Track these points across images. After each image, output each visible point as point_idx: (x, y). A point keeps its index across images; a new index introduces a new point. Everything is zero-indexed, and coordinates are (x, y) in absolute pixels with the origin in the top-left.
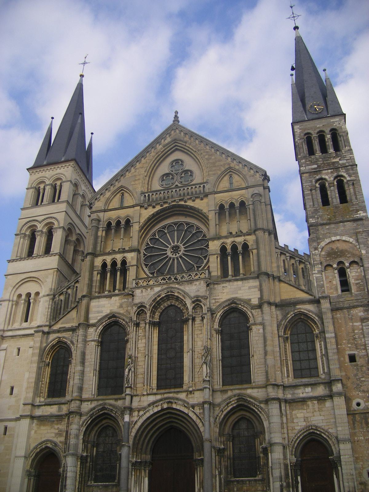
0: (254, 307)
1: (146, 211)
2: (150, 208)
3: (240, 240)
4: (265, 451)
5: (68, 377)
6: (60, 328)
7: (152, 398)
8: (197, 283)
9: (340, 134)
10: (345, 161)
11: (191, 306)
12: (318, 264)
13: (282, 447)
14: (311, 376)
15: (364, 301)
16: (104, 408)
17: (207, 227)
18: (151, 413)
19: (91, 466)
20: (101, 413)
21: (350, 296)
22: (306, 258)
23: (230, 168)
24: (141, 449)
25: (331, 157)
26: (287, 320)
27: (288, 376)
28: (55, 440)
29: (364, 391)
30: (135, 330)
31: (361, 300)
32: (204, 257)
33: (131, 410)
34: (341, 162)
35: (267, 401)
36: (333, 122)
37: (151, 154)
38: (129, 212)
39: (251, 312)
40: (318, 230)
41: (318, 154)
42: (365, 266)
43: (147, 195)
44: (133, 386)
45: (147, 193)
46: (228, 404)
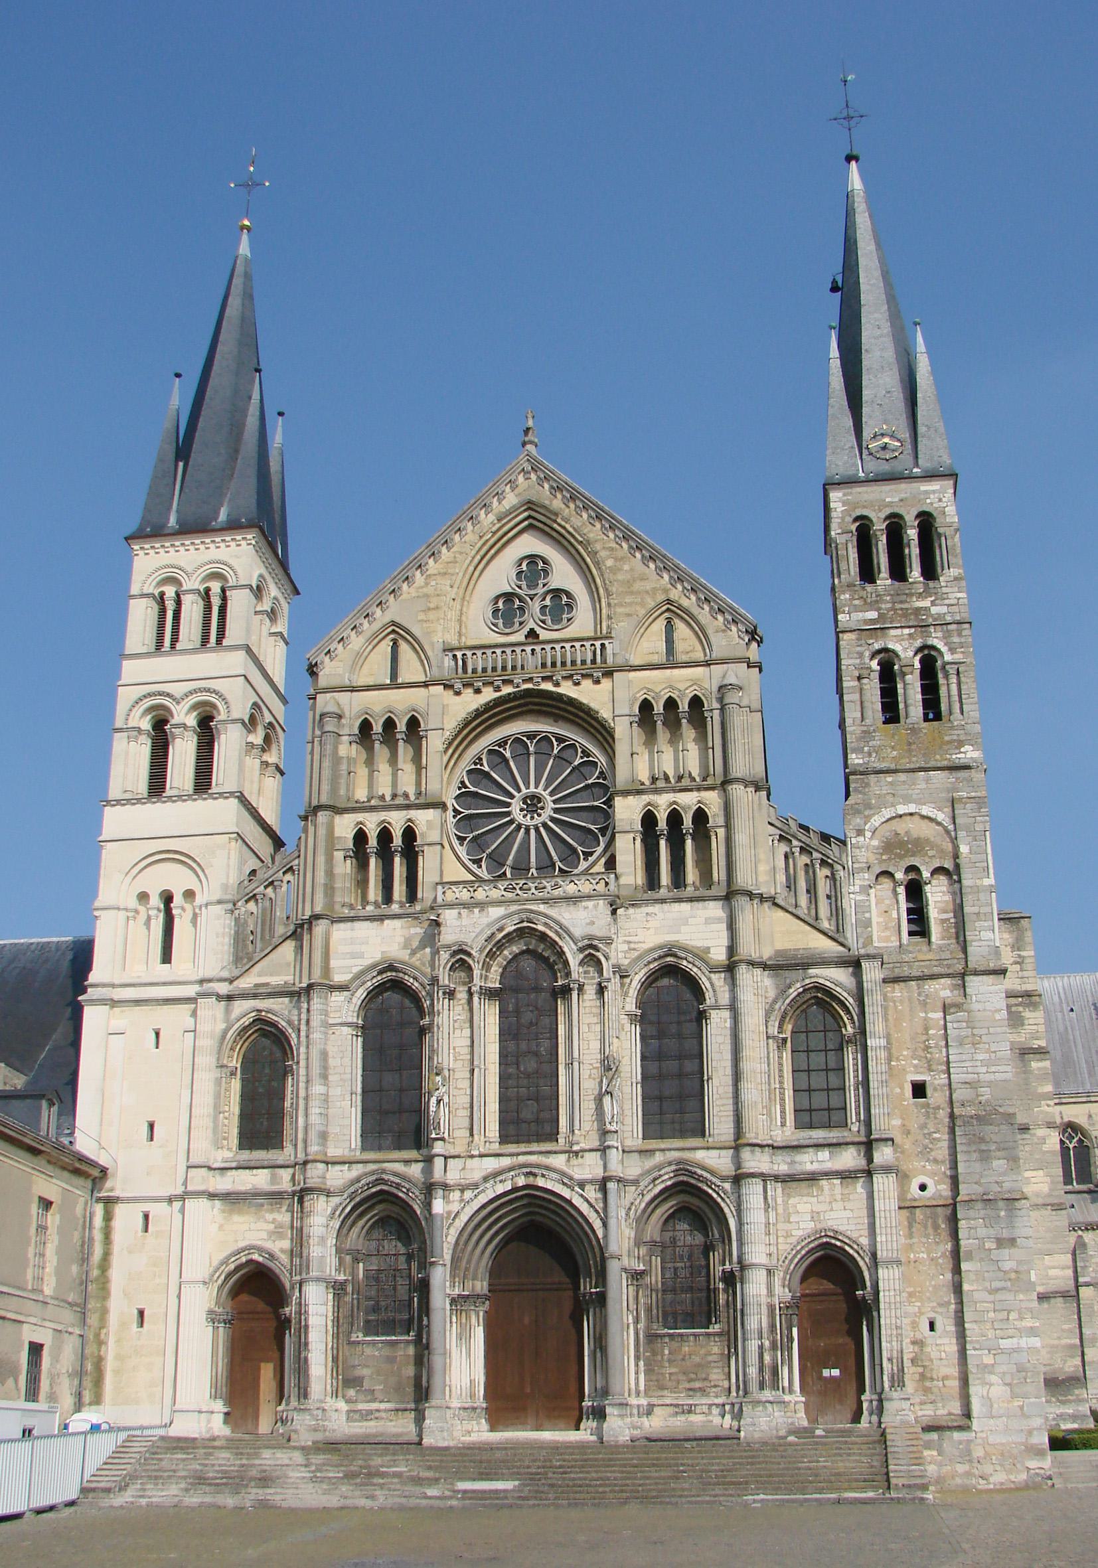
0: (714, 969)
3: (688, 801)
4: (730, 1279)
5: (287, 1104)
6: (257, 985)
7: (491, 1164)
8: (590, 904)
9: (940, 530)
10: (944, 609)
12: (861, 870)
13: (764, 1272)
14: (828, 1126)
15: (954, 965)
16: (380, 1181)
17: (609, 754)
18: (491, 1195)
19: (355, 1302)
20: (374, 1190)
21: (925, 948)
22: (837, 854)
23: (669, 601)
24: (467, 1269)
25: (911, 595)
26: (788, 1001)
27: (783, 1124)
28: (268, 1245)
29: (936, 1161)
30: (446, 1007)
31: (949, 962)
33: (445, 1187)
34: (934, 610)
35: (738, 1179)
36: (926, 492)
37: (466, 538)
38: (416, 697)
39: (709, 979)
40: (868, 785)
41: (884, 579)
42: (965, 882)
43: (459, 654)
44: (446, 1135)
45: (460, 649)
46: (655, 1179)
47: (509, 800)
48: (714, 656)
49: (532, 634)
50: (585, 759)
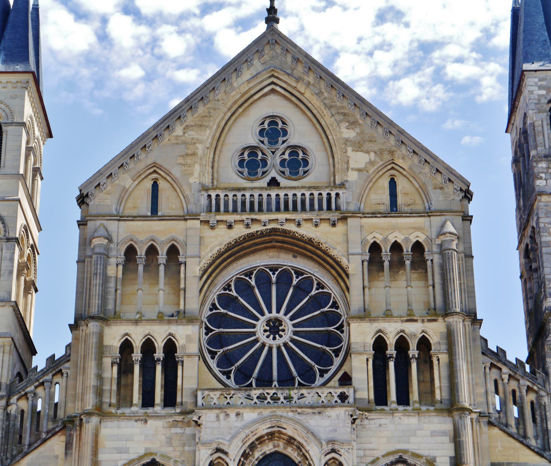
2: (222, 229)
11: (320, 460)
32: (334, 351)
37: (219, 97)
43: (213, 195)
45: (215, 189)
47: (254, 322)
48: (433, 208)
50: (320, 290)
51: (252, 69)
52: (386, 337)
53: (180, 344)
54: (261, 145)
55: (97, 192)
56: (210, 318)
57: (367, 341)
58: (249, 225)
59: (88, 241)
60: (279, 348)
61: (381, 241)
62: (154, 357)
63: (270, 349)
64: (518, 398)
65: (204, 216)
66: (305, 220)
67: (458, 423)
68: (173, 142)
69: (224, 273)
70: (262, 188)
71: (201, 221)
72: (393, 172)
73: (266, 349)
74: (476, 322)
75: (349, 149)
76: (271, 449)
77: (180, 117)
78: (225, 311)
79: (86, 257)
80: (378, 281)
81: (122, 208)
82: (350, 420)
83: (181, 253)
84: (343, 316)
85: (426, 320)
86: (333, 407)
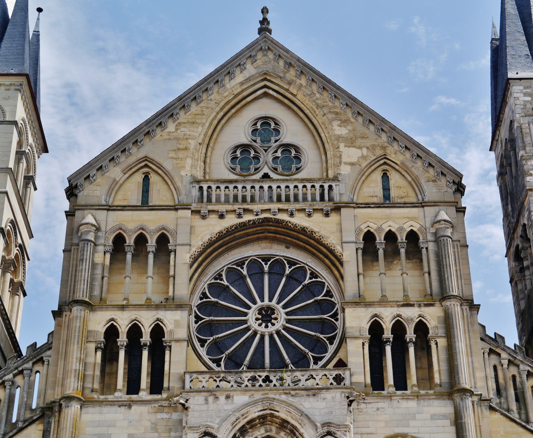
1: (203, 222)
2: (213, 219)
17: (335, 276)
32: (328, 339)
37: (212, 97)
45: (207, 181)
47: (246, 311)
48: (426, 200)
49: (266, 176)
50: (314, 280)
51: (245, 72)
52: (383, 321)
53: (168, 329)
54: (254, 143)
55: (87, 184)
56: (199, 307)
57: (363, 326)
58: (241, 215)
59: (75, 229)
60: (271, 336)
61: (375, 230)
62: (140, 342)
63: (262, 337)
64: (518, 384)
65: (194, 206)
66: (299, 210)
67: (459, 404)
68: (165, 137)
69: (215, 263)
70: (254, 181)
71: (192, 211)
72: (385, 167)
73: (258, 336)
74: (474, 308)
75: (342, 145)
76: (263, 434)
77: (172, 115)
78: (216, 300)
79: (72, 245)
80: (373, 270)
81: (111, 199)
82: (346, 402)
83: (171, 241)
84: (337, 305)
85: (423, 305)
86: (328, 389)
